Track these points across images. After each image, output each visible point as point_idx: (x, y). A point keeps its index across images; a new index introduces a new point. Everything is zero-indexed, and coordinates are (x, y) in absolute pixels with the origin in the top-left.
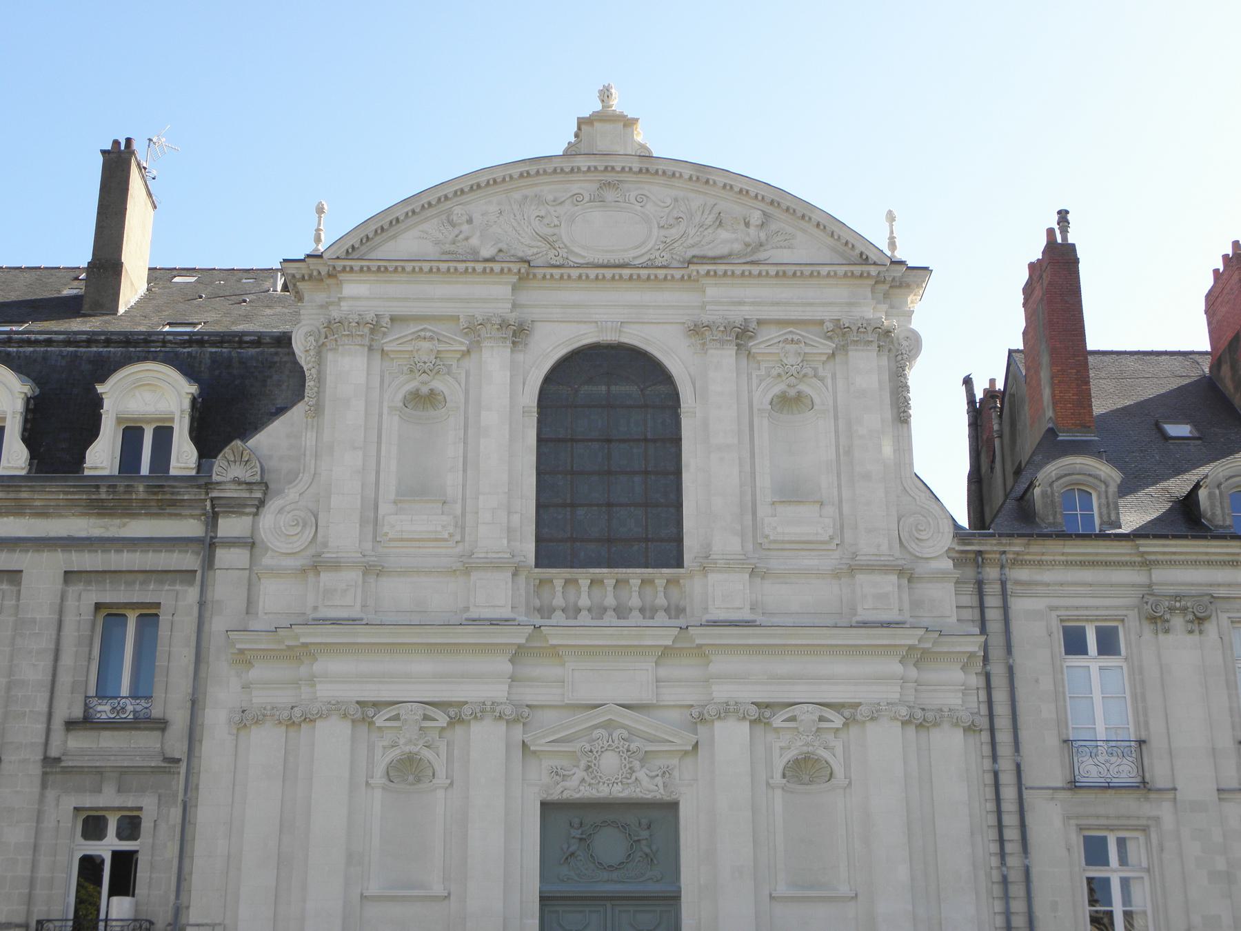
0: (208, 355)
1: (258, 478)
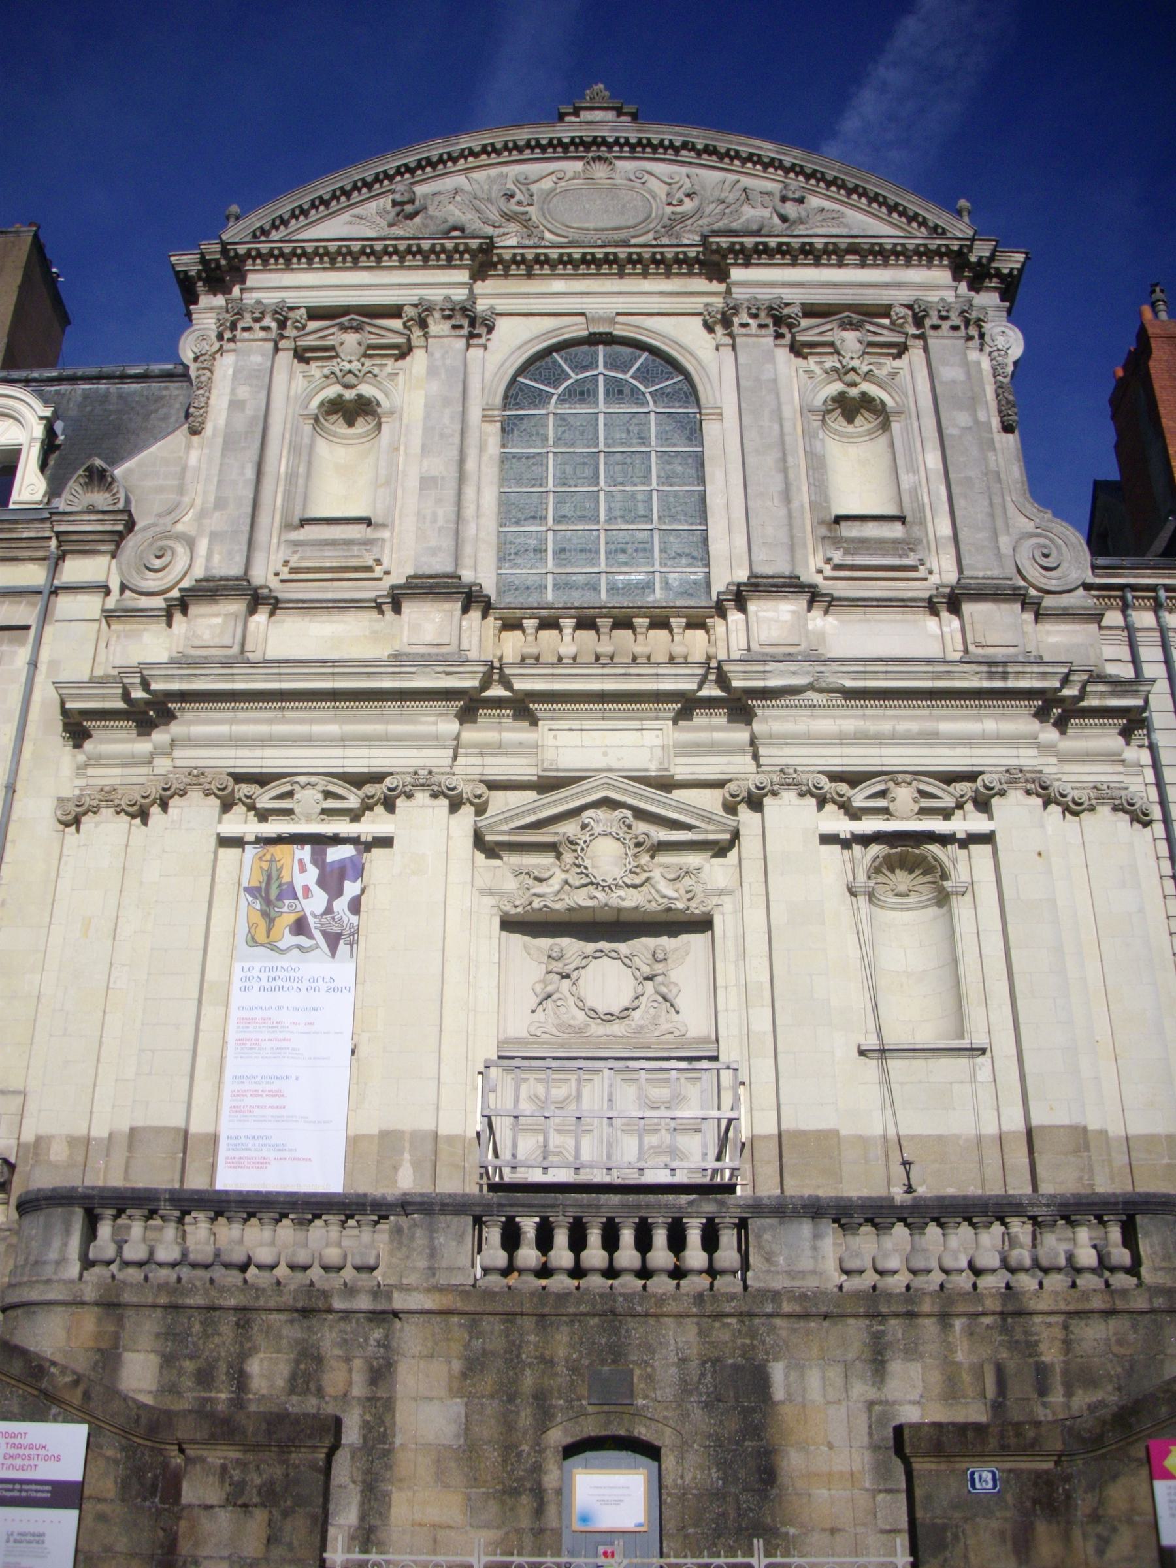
0: (80, 392)
1: (121, 505)
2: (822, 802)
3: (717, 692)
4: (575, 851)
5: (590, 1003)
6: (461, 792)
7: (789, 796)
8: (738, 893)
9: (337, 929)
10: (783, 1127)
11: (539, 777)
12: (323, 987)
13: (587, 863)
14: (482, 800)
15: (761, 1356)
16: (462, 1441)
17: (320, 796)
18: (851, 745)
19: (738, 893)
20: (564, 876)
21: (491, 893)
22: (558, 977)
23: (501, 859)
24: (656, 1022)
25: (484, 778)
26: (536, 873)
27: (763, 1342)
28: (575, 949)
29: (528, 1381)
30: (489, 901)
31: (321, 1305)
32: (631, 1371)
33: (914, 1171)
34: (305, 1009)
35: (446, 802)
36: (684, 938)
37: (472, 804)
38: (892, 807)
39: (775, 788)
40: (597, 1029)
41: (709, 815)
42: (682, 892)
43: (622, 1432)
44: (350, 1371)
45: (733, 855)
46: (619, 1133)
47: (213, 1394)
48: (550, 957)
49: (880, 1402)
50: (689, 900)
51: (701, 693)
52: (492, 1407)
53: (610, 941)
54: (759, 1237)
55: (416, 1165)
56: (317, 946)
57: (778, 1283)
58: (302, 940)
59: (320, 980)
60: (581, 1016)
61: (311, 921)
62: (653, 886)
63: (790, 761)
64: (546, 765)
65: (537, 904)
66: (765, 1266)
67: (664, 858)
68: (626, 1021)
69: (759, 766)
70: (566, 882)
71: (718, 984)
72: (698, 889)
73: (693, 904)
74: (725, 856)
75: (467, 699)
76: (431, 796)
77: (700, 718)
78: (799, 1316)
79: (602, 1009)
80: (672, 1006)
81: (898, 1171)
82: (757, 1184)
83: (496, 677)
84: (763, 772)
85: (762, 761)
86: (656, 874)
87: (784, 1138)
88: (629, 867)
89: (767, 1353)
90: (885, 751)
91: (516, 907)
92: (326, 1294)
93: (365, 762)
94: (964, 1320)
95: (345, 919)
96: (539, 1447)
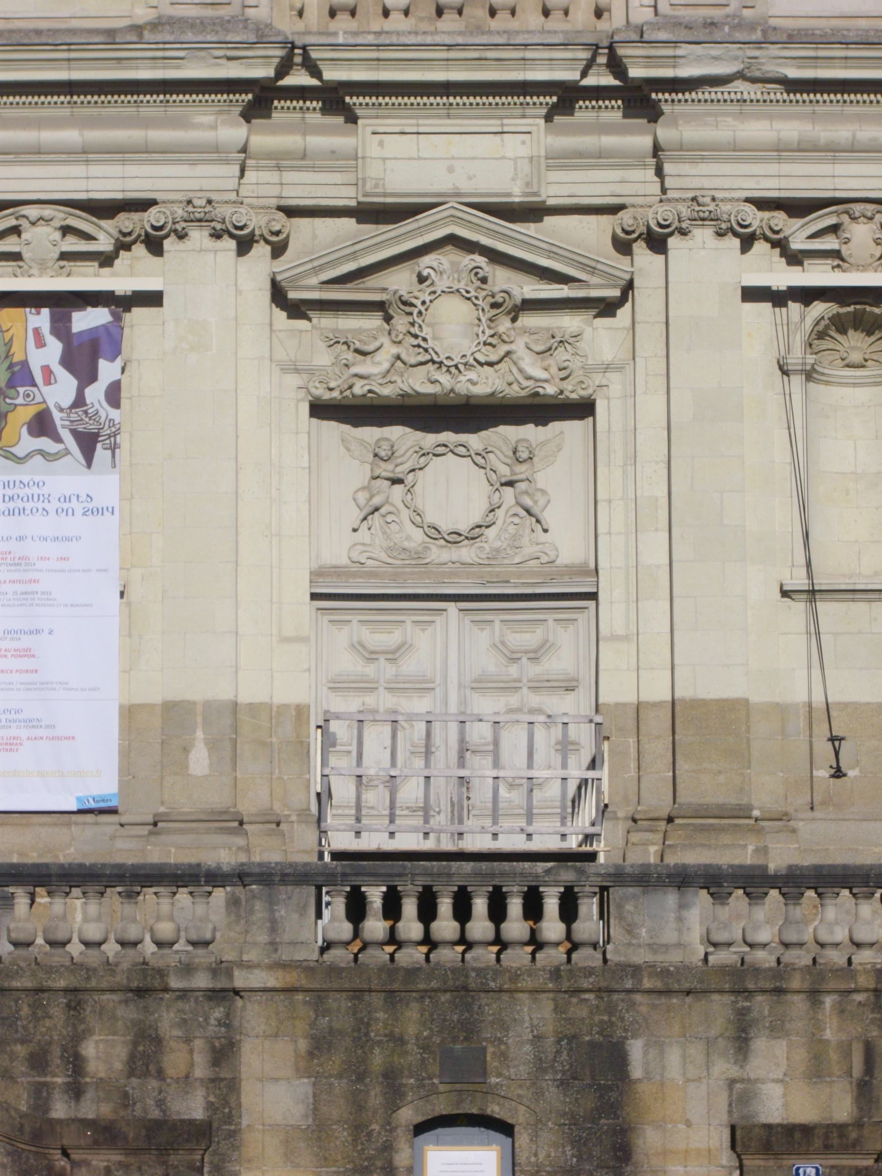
2: (747, 242)
3: (609, 80)
4: (411, 314)
5: (431, 517)
6: (253, 231)
7: (703, 235)
8: (629, 369)
9: (92, 427)
10: (678, 695)
11: (359, 203)
12: (79, 508)
13: (426, 332)
14: (282, 237)
15: (619, 1033)
16: (310, 1121)
17: (57, 235)
18: (793, 160)
19: (629, 369)
20: (394, 350)
21: (297, 371)
22: (387, 483)
23: (310, 320)
24: (517, 544)
25: (283, 202)
26: (358, 345)
27: (622, 1019)
28: (409, 444)
29: (377, 1059)
30: (293, 380)
31: (157, 984)
32: (484, 1049)
33: (846, 750)
34: (56, 539)
35: (232, 244)
36: (556, 426)
37: (267, 242)
38: (845, 252)
39: (684, 225)
40: (439, 554)
41: (593, 264)
42: (554, 370)
43: (475, 1111)
44: (191, 1051)
45: (624, 312)
46: (468, 691)
47: (48, 1079)
48: (376, 455)
49: (742, 1081)
50: (562, 379)
51: (586, 82)
52: (340, 1086)
53: (457, 431)
54: (620, 907)
55: (212, 745)
56: (67, 452)
57: (640, 957)
58: (45, 443)
59: (74, 499)
60: (418, 535)
61: (57, 416)
62: (515, 363)
63: (707, 183)
64: (369, 187)
65: (358, 390)
66: (626, 939)
67: (528, 320)
68: (478, 543)
69: (664, 191)
70: (398, 358)
71: (599, 497)
72: (575, 364)
73: (568, 386)
74: (613, 315)
75: (257, 90)
76: (212, 235)
77: (584, 113)
78: (660, 992)
79: (445, 526)
80: (538, 521)
81: (824, 749)
82: (643, 765)
83: (298, 59)
84: (669, 200)
85: (669, 182)
86: (518, 346)
87: (678, 709)
88: (482, 339)
89: (626, 1030)
90: (841, 169)
91: (331, 389)
92: (161, 973)
93: (118, 185)
94: (835, 997)
95: (103, 414)
96: (389, 1127)
